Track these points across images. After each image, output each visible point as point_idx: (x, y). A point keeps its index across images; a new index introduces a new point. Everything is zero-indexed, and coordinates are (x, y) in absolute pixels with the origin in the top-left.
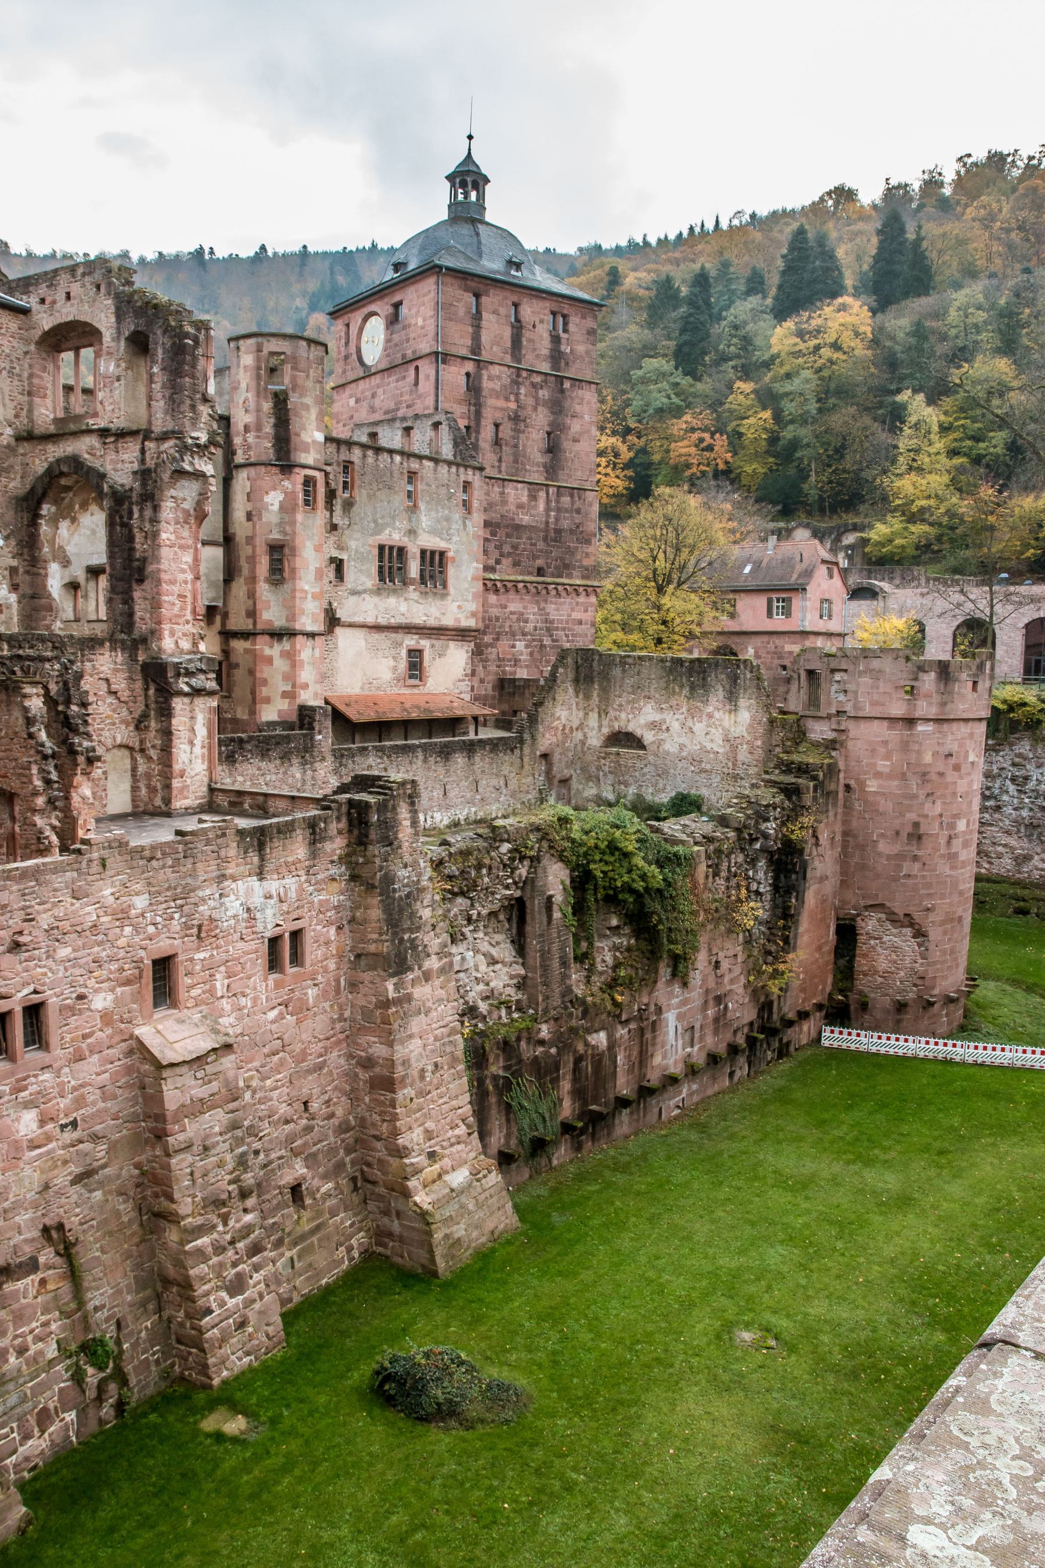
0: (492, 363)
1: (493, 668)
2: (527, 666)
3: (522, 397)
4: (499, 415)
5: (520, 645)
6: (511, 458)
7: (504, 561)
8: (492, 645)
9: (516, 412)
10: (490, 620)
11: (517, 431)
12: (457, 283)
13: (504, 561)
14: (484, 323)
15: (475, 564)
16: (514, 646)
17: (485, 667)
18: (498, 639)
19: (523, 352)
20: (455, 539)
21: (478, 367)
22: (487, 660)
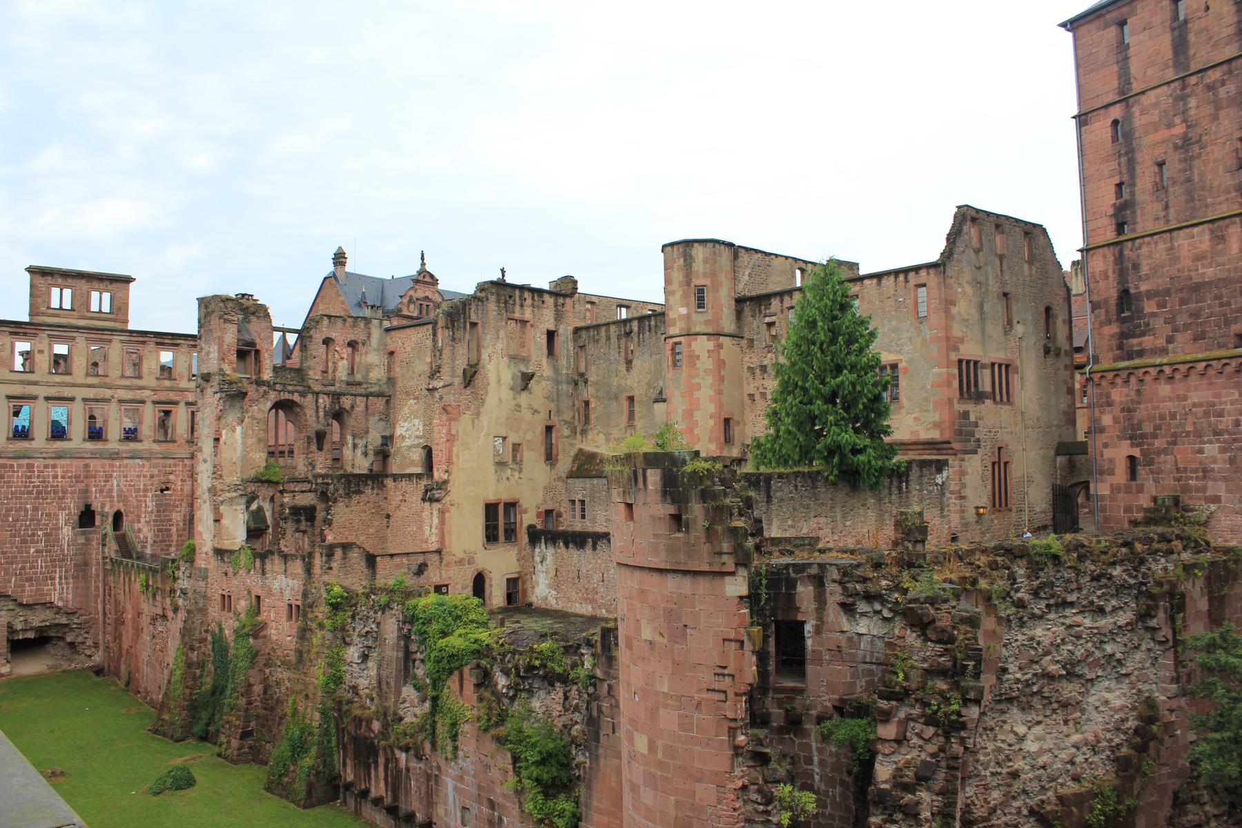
0: (1143, 92)
1: (1168, 482)
2: (1225, 479)
3: (1192, 112)
4: (1159, 154)
5: (1211, 449)
6: (1183, 198)
7: (1179, 337)
8: (1165, 451)
9: (1186, 134)
10: (1162, 417)
11: (1189, 160)
12: (1092, 26)
13: (1179, 337)
14: (1132, 51)
15: (936, 370)
16: (1201, 451)
17: (1156, 481)
18: (1174, 443)
19: (1192, 52)
20: (906, 349)
21: (1128, 106)
22: (1159, 472)
